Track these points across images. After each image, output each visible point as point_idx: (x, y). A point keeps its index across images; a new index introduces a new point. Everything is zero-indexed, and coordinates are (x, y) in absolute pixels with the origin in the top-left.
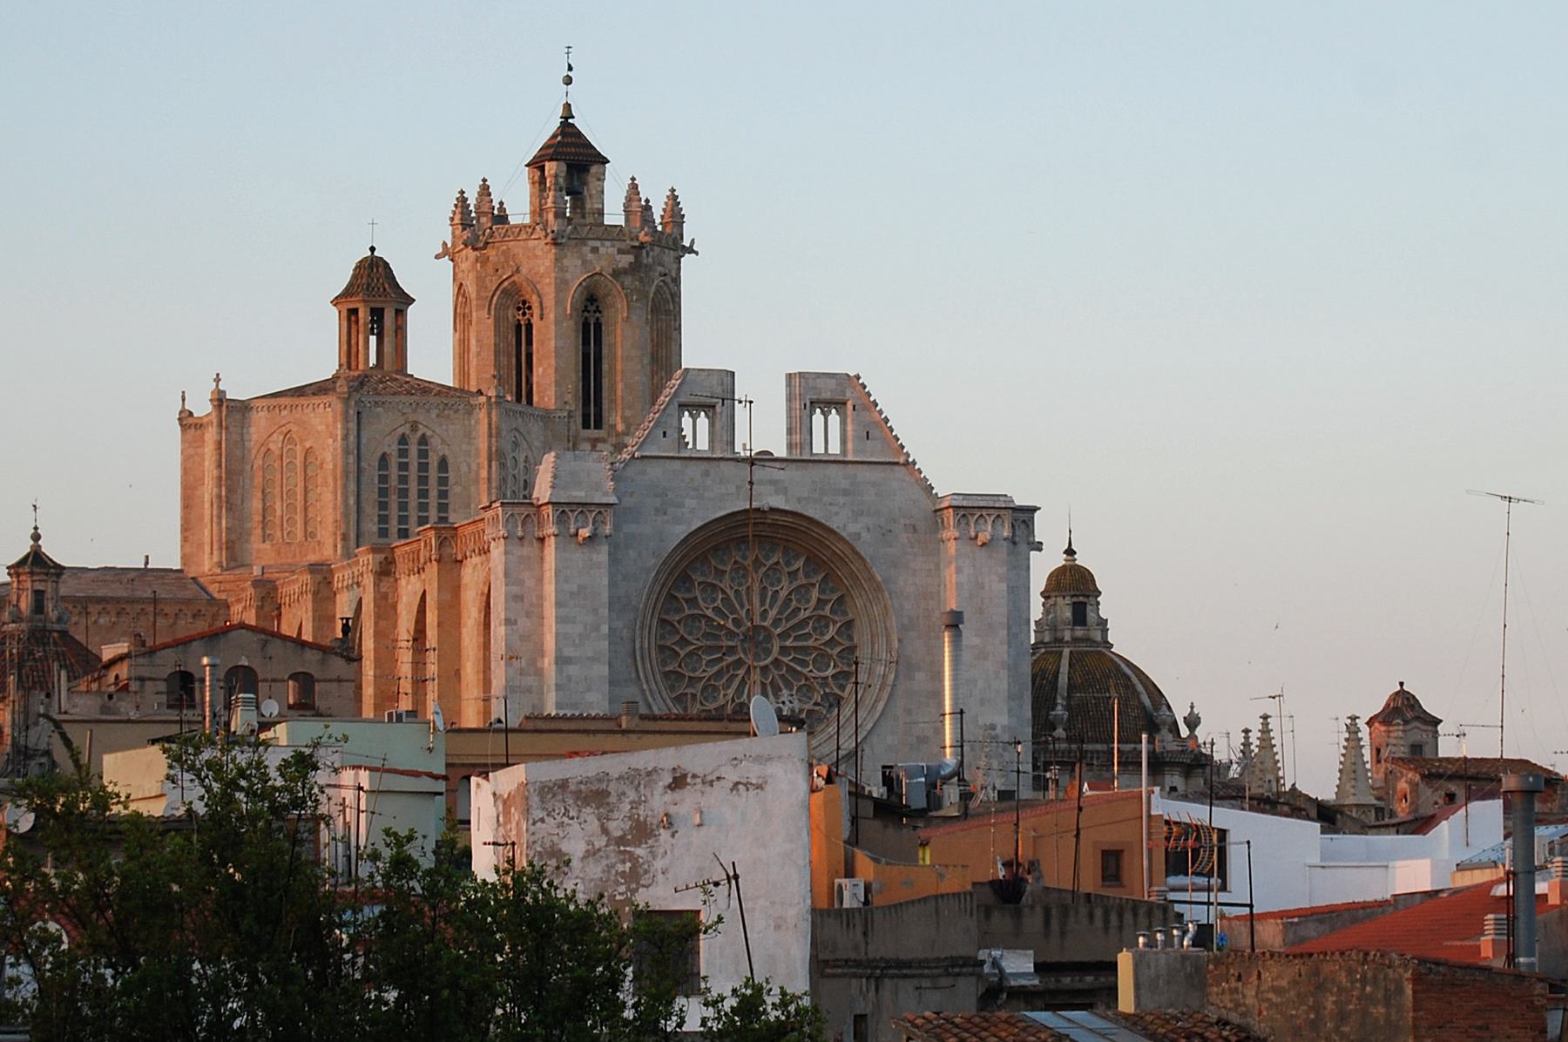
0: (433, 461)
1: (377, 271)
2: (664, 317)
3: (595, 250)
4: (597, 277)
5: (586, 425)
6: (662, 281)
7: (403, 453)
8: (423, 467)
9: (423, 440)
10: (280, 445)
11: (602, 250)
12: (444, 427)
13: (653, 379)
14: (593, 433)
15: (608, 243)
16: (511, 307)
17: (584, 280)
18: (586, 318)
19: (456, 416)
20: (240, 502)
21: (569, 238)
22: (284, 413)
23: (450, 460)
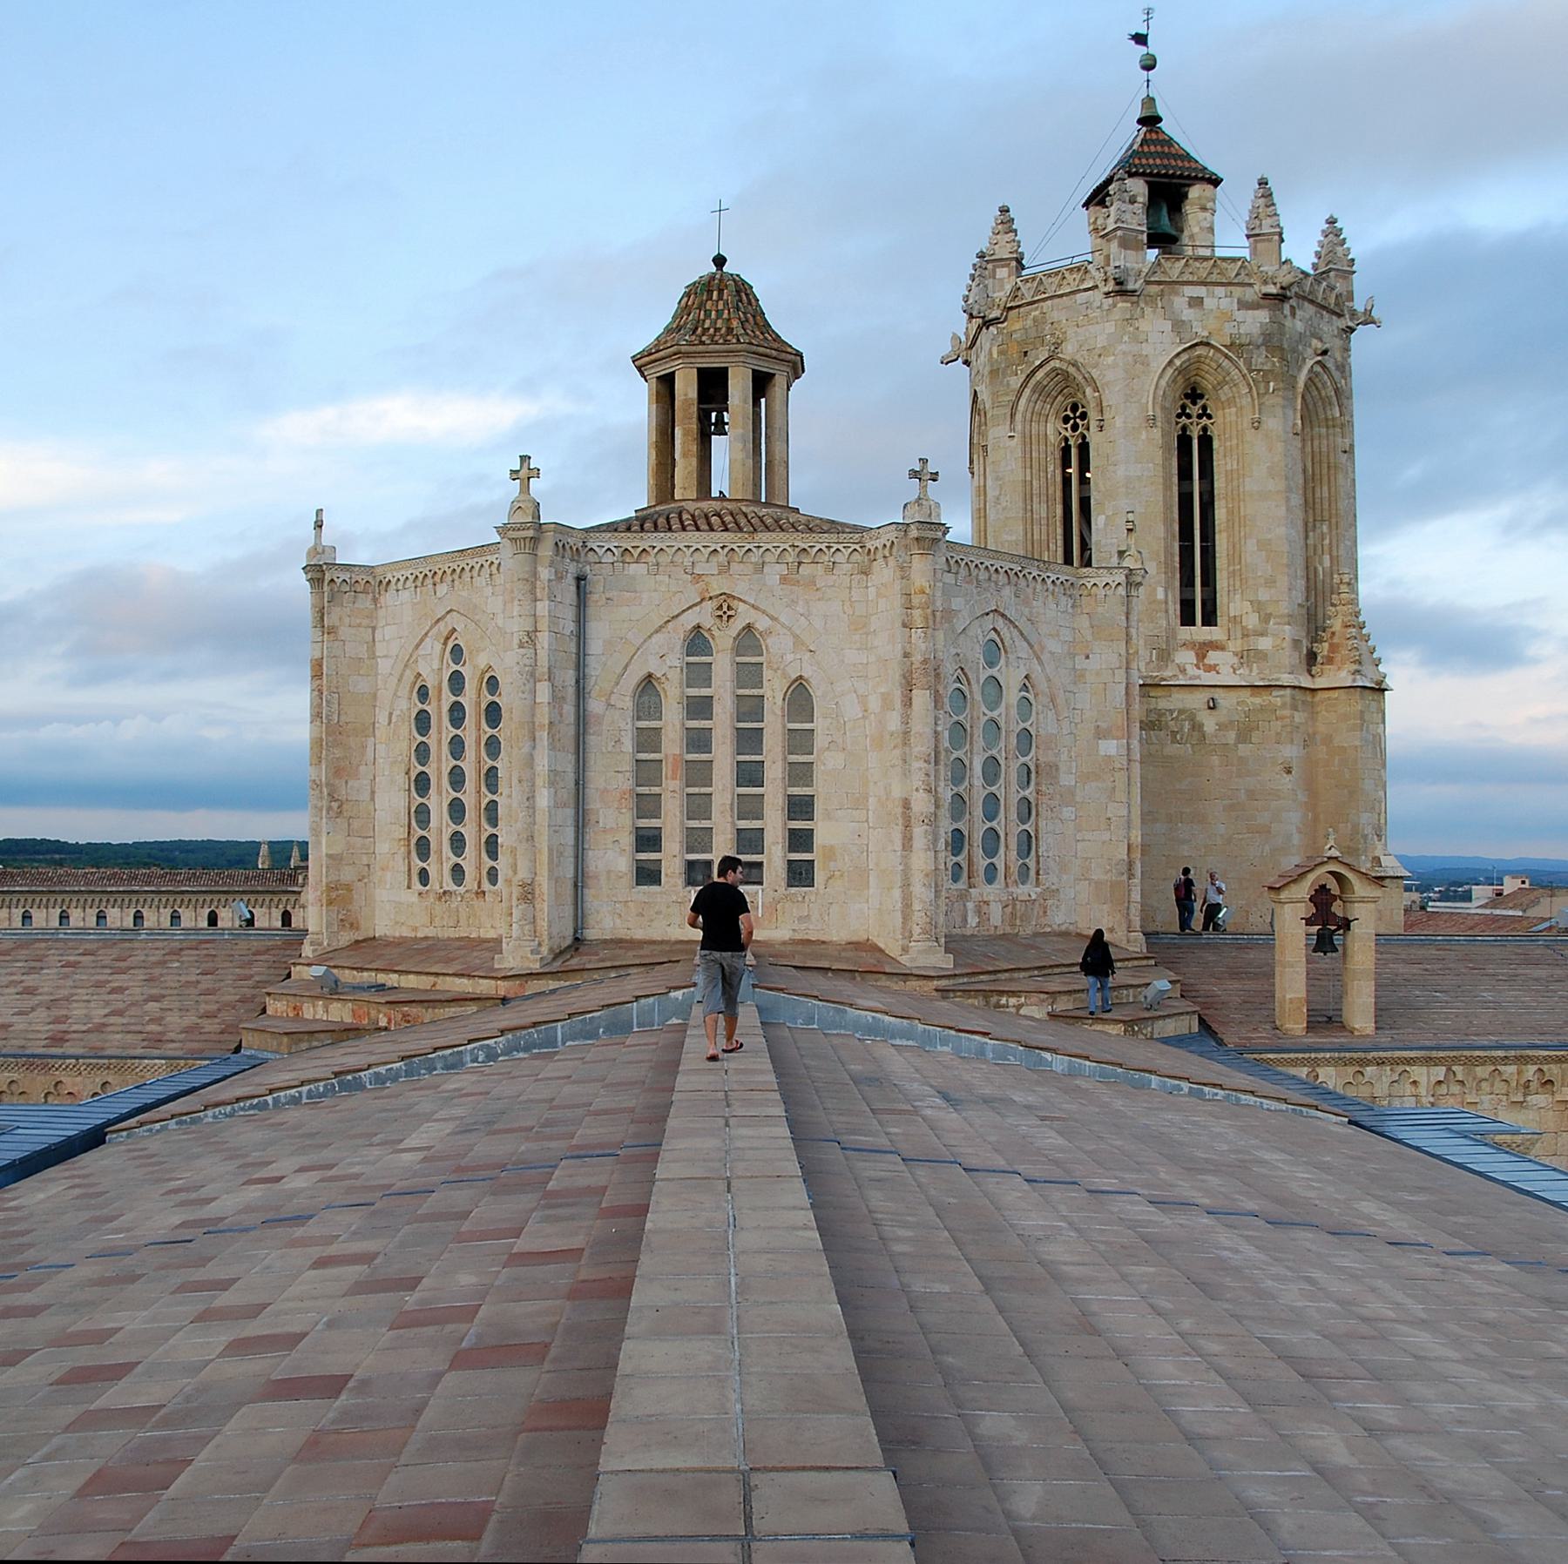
0: (774, 692)
1: (720, 297)
2: (1323, 431)
3: (1196, 302)
4: (1200, 351)
5: (1187, 619)
6: (1318, 362)
7: (699, 674)
8: (751, 708)
9: (748, 639)
10: (436, 666)
11: (1209, 303)
12: (800, 609)
13: (1307, 537)
14: (1200, 632)
15: (1220, 291)
16: (1051, 418)
17: (1178, 355)
18: (1184, 428)
19: (831, 579)
20: (366, 796)
21: (1148, 283)
22: (442, 589)
23: (817, 691)
